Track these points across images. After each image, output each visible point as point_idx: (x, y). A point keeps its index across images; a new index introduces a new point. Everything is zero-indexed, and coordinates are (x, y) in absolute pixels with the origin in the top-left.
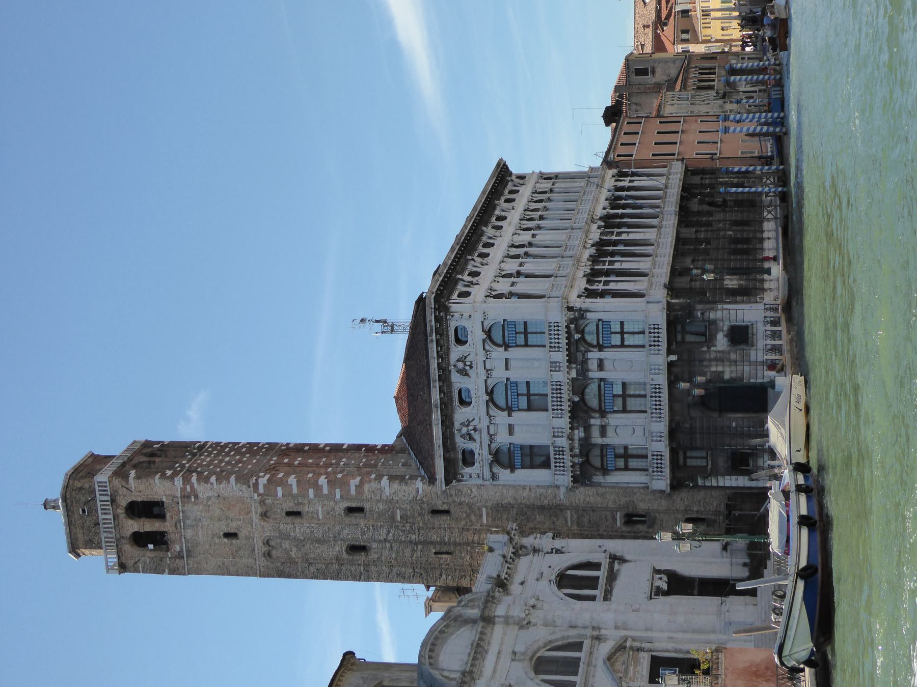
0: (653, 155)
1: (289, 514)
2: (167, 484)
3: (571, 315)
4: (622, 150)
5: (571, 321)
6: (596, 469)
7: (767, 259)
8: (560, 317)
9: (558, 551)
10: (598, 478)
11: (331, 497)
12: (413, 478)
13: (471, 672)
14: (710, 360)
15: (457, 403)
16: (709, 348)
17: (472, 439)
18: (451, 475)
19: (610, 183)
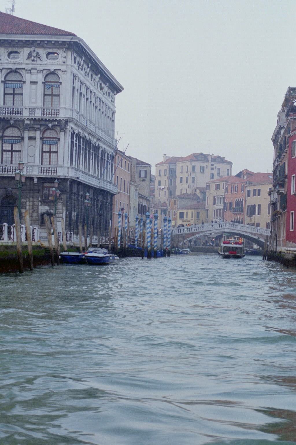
0: (118, 176)
5: (59, 121)
8: (63, 115)
14: (33, 202)
15: (11, 50)
16: (40, 201)
19: (110, 151)
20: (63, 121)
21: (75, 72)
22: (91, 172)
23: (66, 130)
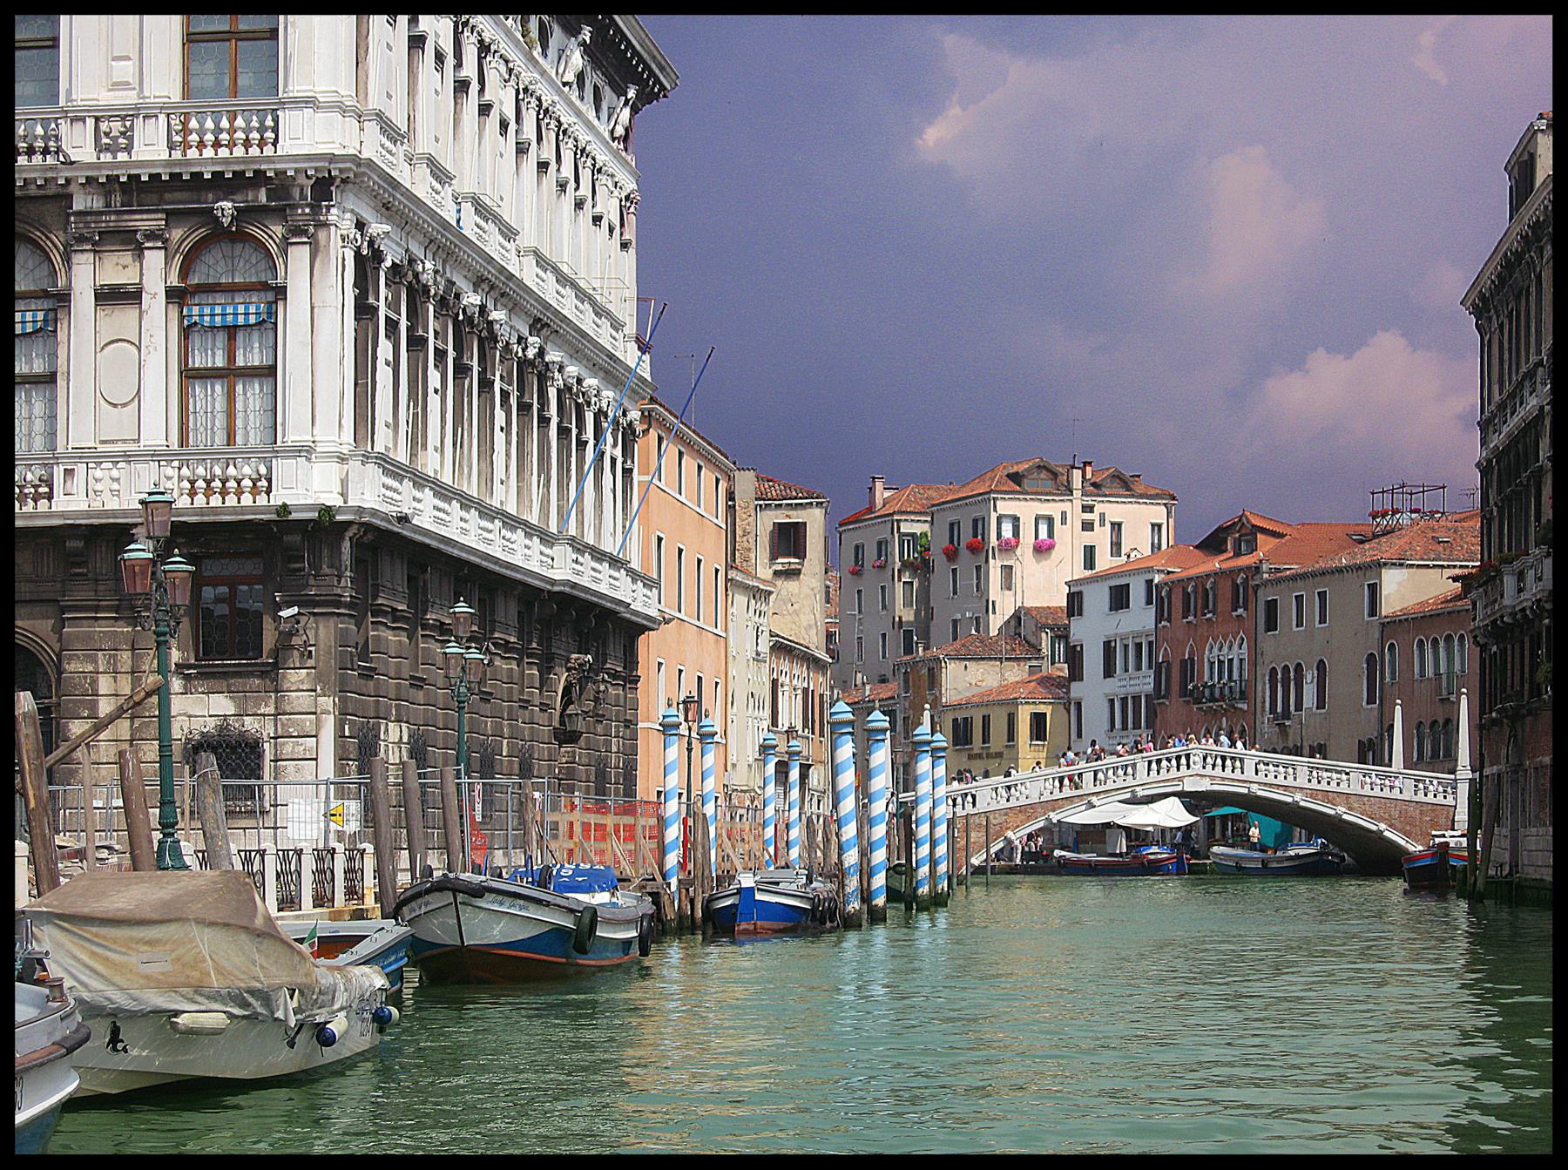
5: (280, 186)
20: (302, 180)
23: (322, 235)
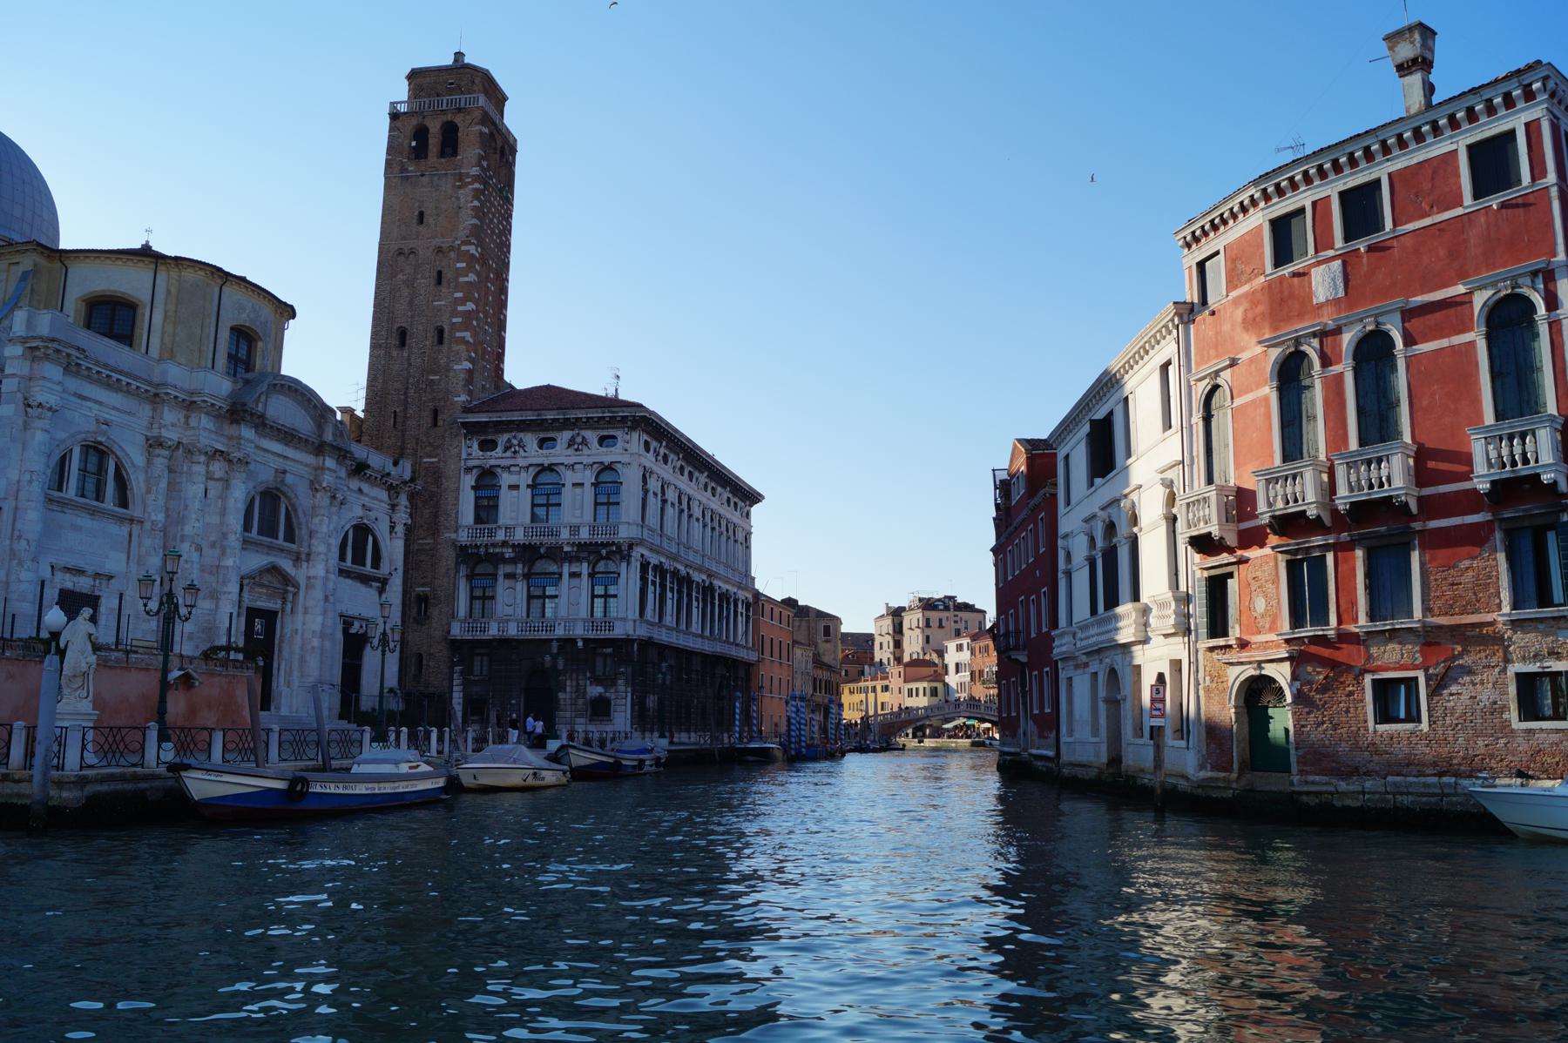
1: (440, 273)
2: (474, 161)
3: (624, 548)
4: (767, 607)
5: (619, 546)
6: (473, 569)
7: (672, 736)
8: (625, 533)
9: (392, 528)
10: (463, 571)
11: (454, 313)
12: (470, 393)
13: (264, 425)
17: (506, 449)
18: (472, 429)
19: (742, 595)
21: (648, 464)
22: (696, 627)
